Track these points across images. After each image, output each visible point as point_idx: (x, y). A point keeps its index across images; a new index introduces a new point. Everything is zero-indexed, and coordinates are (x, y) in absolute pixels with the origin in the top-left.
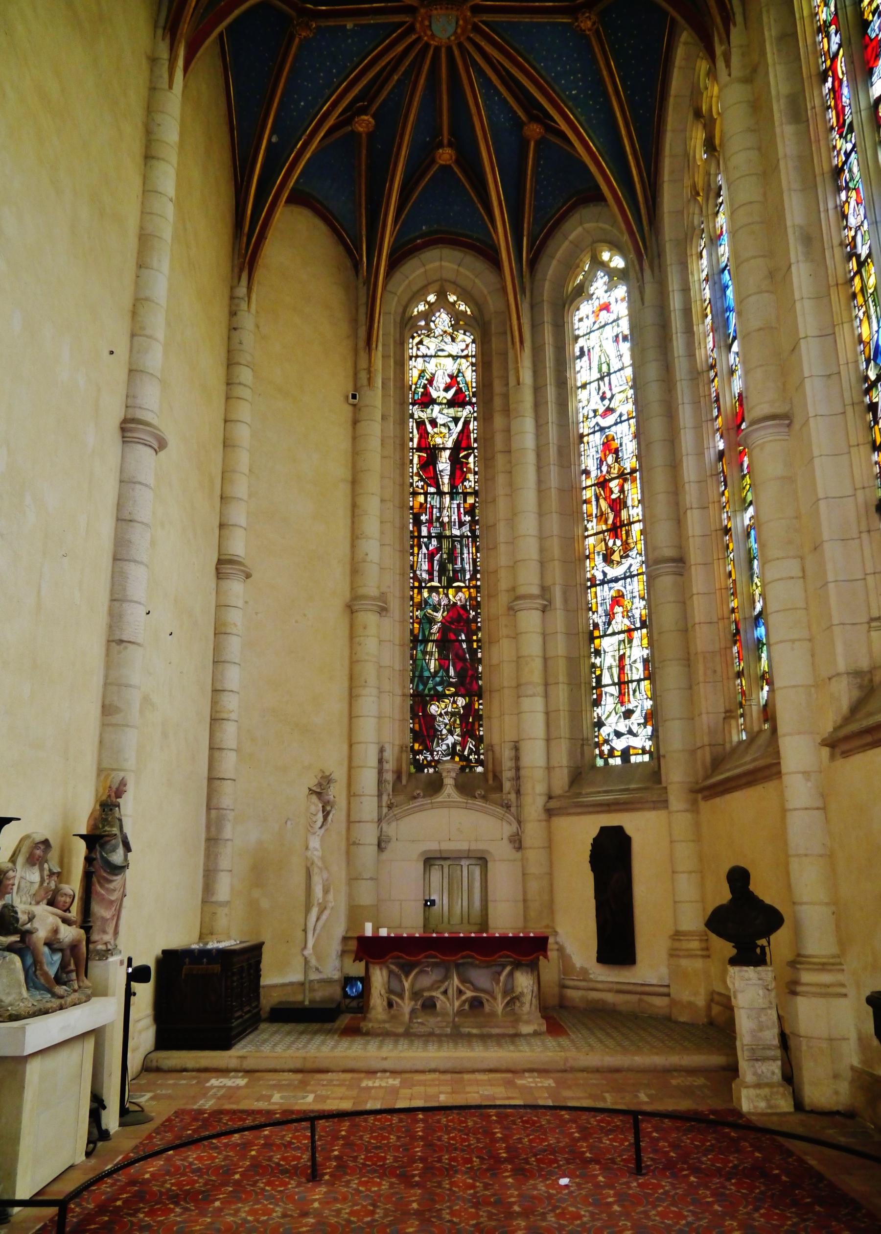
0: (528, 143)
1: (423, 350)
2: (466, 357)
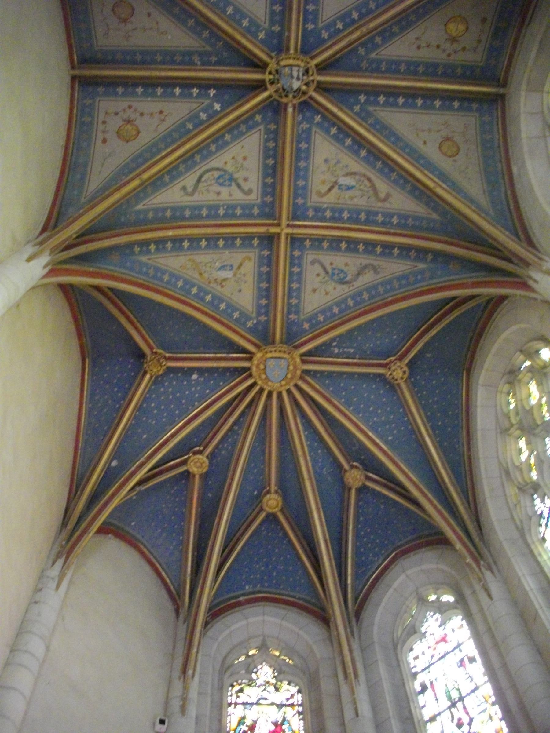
0: (350, 489)
1: (243, 698)
2: (292, 705)
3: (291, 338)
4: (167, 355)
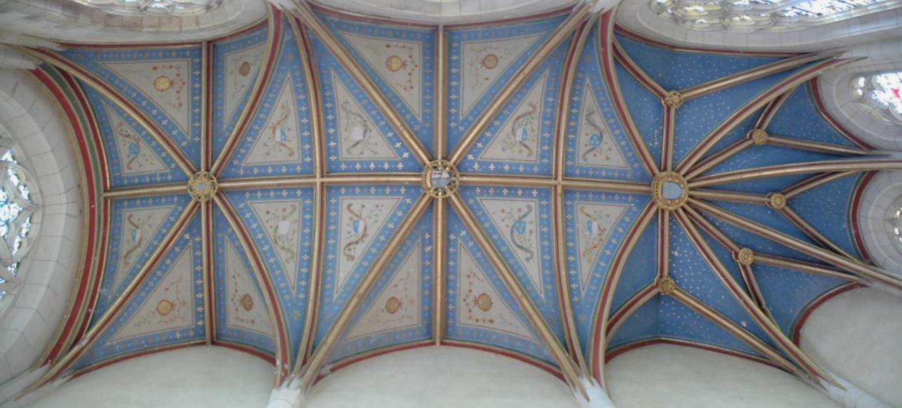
3: (648, 179)
4: (659, 275)
